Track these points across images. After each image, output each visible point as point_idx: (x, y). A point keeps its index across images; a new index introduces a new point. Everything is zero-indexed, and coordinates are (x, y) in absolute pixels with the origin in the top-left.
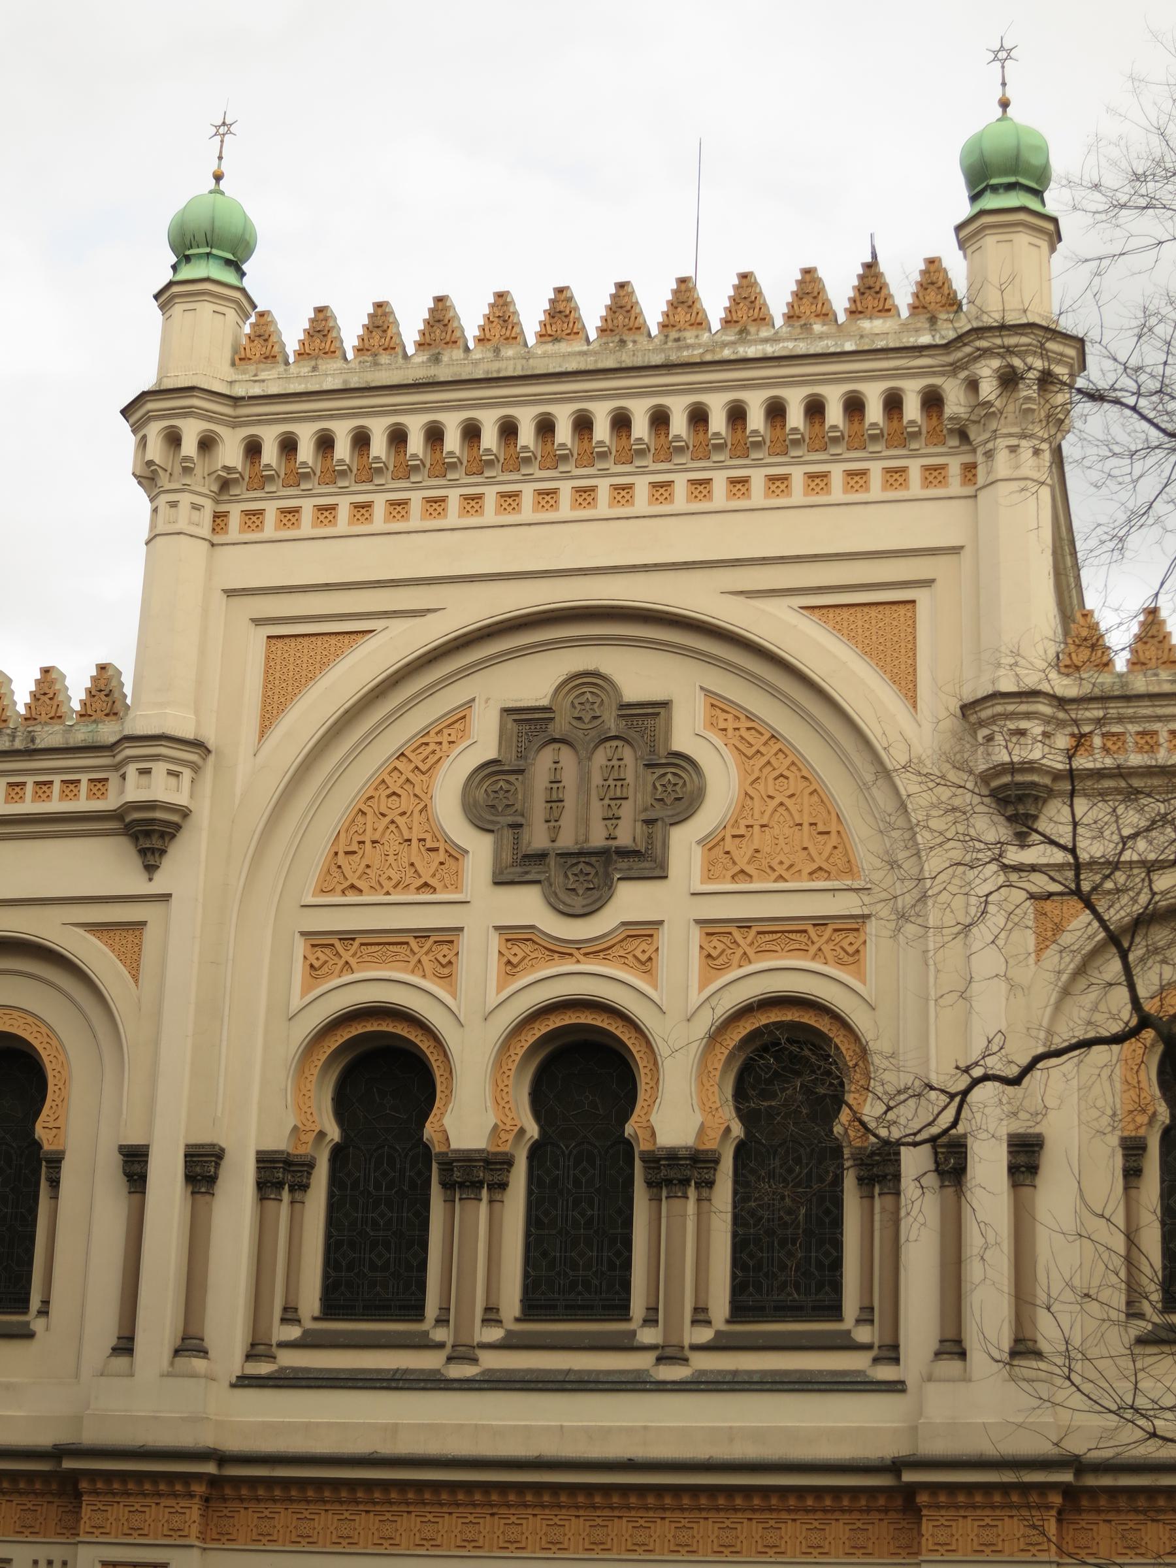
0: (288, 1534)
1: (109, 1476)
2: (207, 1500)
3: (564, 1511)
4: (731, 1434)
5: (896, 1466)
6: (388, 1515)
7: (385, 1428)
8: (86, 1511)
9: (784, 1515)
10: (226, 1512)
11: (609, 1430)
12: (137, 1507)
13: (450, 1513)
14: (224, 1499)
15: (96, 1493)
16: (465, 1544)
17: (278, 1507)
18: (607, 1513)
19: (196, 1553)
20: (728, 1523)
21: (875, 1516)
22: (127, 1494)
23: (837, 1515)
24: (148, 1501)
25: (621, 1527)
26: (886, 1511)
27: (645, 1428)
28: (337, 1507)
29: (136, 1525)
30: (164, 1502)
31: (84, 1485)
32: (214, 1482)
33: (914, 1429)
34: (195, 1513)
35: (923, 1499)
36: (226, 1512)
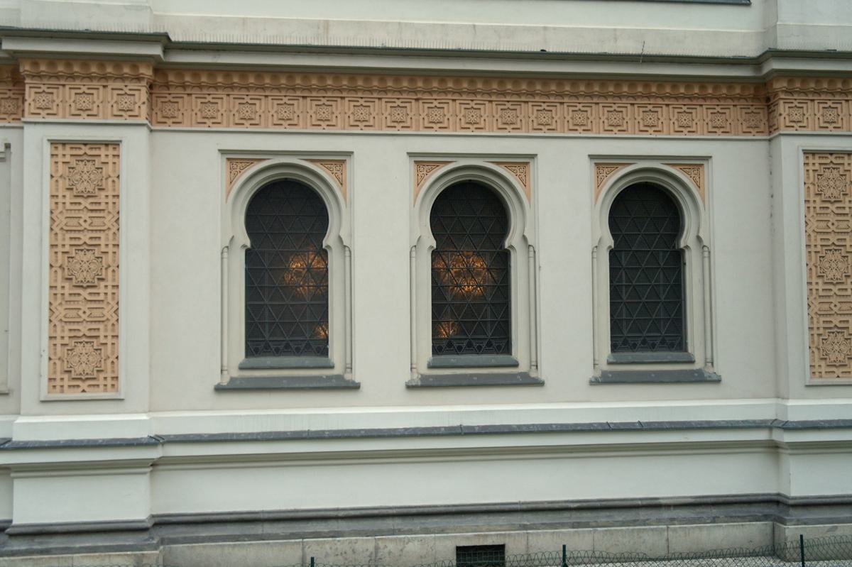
0: (231, 117)
1: (52, 58)
2: (151, 87)
3: (479, 97)
4: (615, 34)
5: (756, 62)
6: (324, 101)
7: (317, 24)
8: (30, 94)
9: (660, 101)
10: (170, 98)
11: (516, 28)
12: (84, 89)
13: (380, 99)
14: (167, 86)
15: (39, 76)
16: (395, 124)
17: (221, 93)
18: (515, 98)
19: (144, 131)
20: (615, 107)
21: (730, 102)
22: (72, 77)
23: (700, 102)
24: (95, 83)
25: (527, 111)
26: (739, 99)
27: (545, 28)
28: (276, 93)
29: (85, 106)
30: (111, 84)
31: (26, 68)
32: (160, 68)
33: (769, 30)
34: (143, 95)
35: (780, 85)
36: (170, 98)
